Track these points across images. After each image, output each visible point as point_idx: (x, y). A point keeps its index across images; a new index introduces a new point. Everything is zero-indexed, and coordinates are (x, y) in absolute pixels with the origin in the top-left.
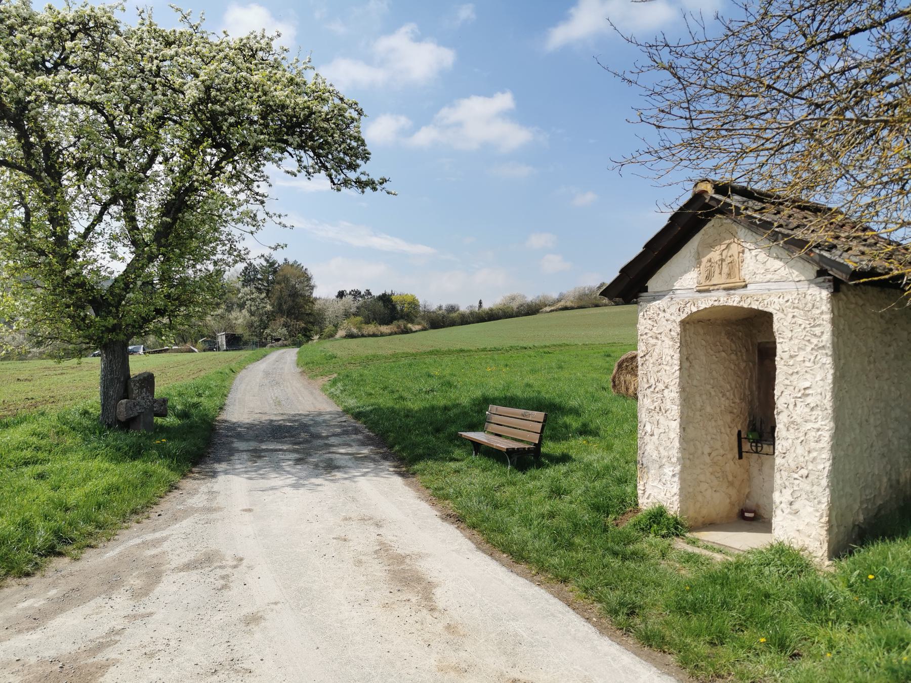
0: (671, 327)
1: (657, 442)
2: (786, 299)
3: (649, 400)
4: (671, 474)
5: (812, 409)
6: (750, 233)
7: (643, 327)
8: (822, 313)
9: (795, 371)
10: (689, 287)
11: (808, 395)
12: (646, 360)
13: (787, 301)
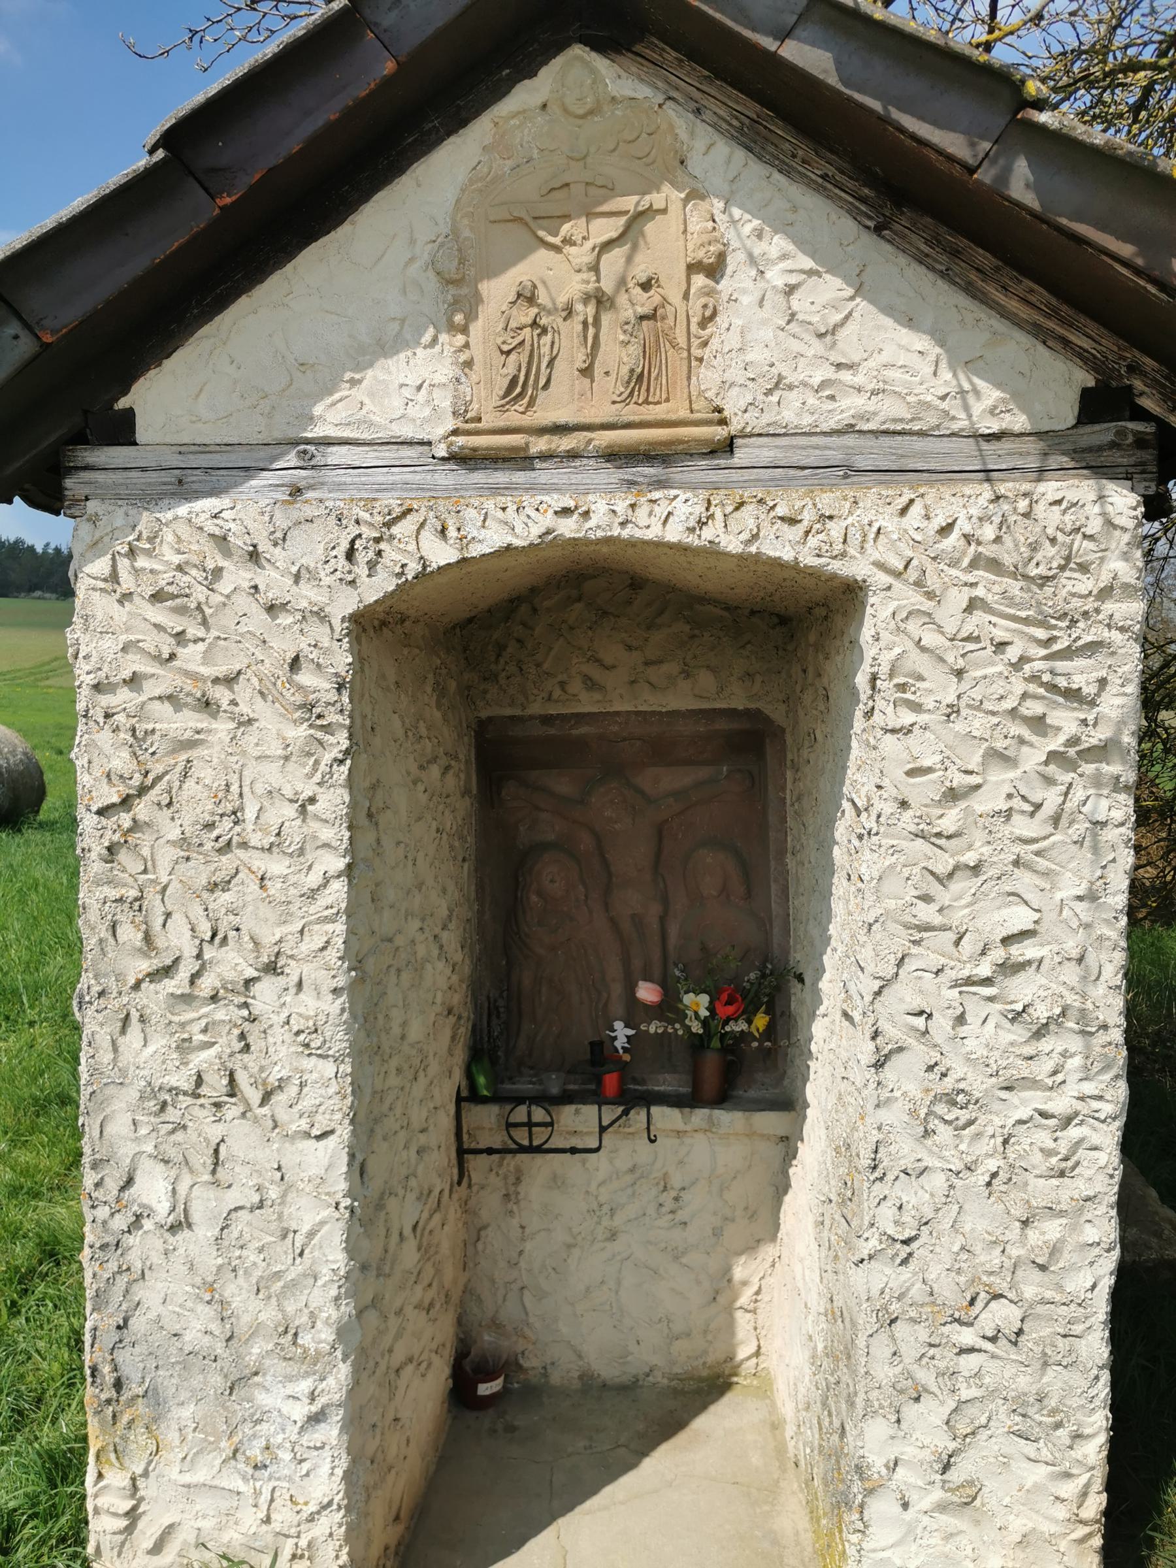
0: (303, 644)
1: (210, 1261)
2: (940, 521)
3: (158, 1043)
4: (300, 1411)
5: (1040, 1032)
6: (756, 170)
7: (109, 645)
8: (1105, 593)
9: (970, 858)
10: (407, 431)
11: (1021, 966)
12: (136, 826)
13: (946, 530)
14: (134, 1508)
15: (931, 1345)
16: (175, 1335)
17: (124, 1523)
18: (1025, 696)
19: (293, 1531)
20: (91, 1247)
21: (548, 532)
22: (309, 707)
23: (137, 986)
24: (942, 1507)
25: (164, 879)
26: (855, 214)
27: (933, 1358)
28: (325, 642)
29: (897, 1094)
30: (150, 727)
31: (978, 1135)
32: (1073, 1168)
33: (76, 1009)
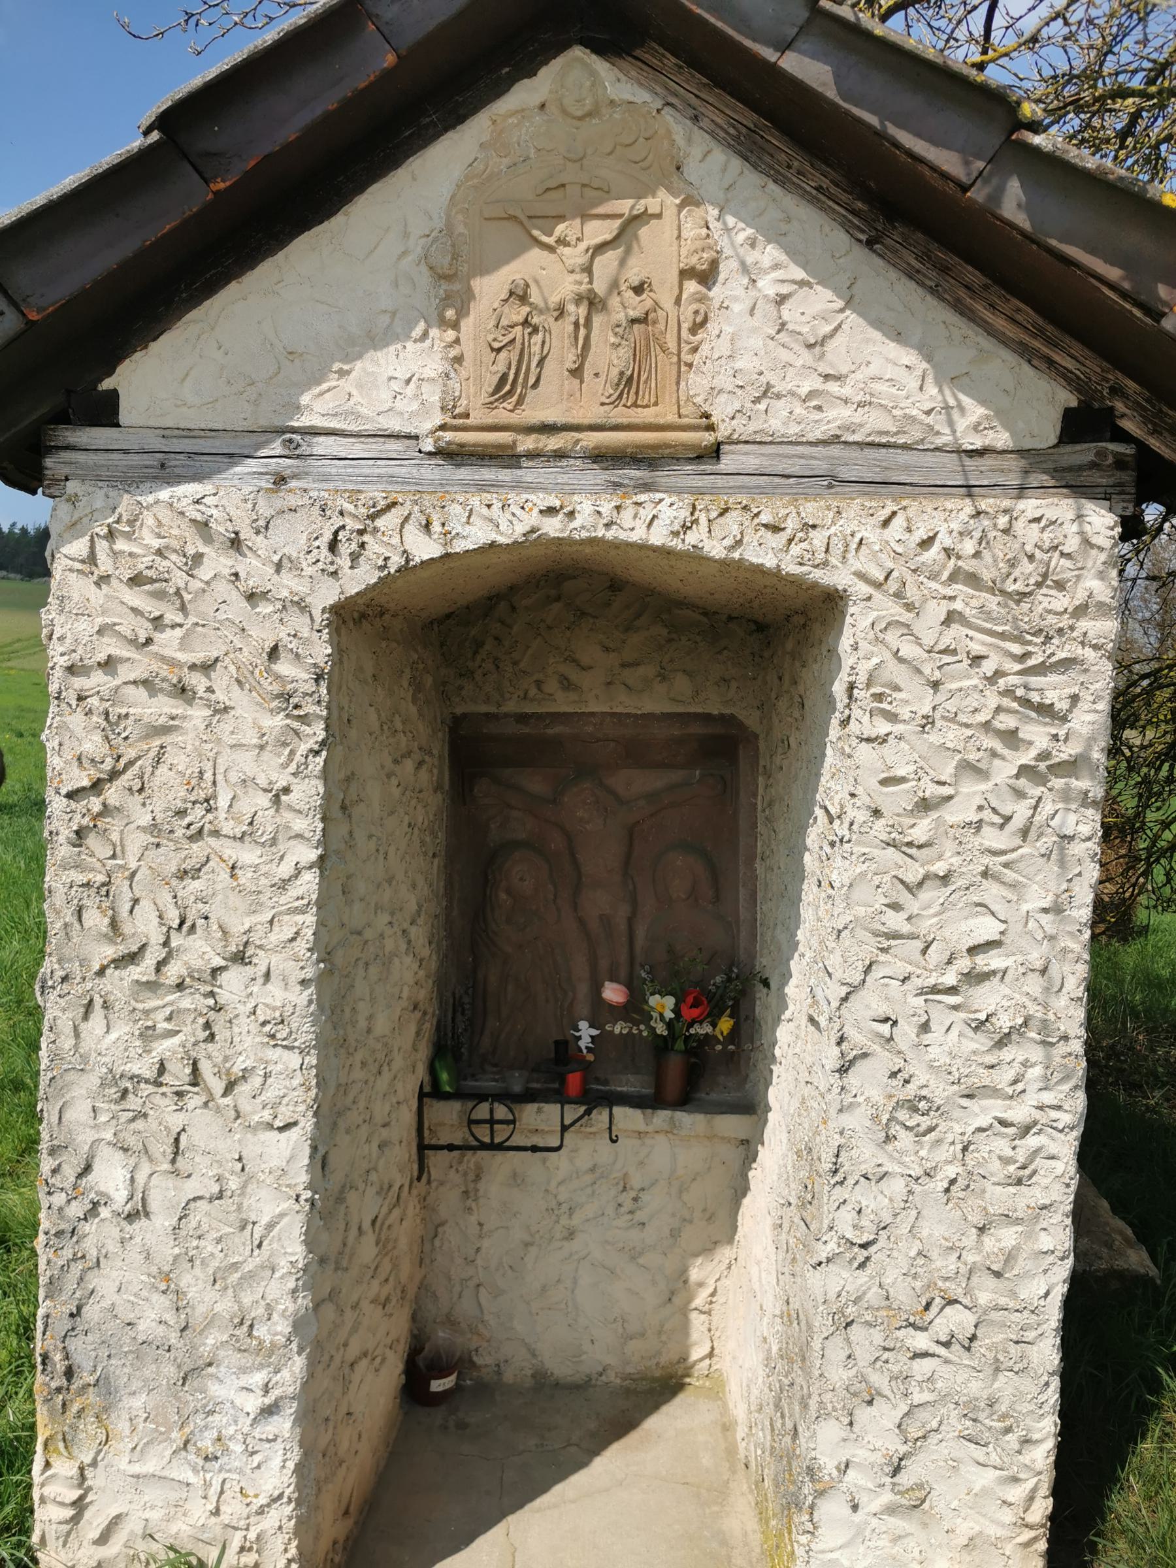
0: (283, 634)
1: (167, 1250)
2: (921, 534)
3: (121, 1030)
4: (253, 1403)
5: (1002, 1042)
6: (752, 178)
7: (85, 627)
8: (1080, 611)
9: (940, 868)
10: (394, 424)
12: (106, 810)
13: (926, 543)
14: (81, 1498)
15: (886, 1349)
16: (129, 1324)
17: (70, 1512)
18: (999, 709)
19: (242, 1524)
20: (46, 1233)
21: (533, 531)
22: (286, 697)
23: (101, 972)
24: (891, 1510)
25: (133, 865)
26: (847, 227)
27: (887, 1362)
28: (305, 632)
29: (860, 1099)
30: (124, 711)
31: (939, 1142)
32: (1030, 1177)
33: (38, 994)
